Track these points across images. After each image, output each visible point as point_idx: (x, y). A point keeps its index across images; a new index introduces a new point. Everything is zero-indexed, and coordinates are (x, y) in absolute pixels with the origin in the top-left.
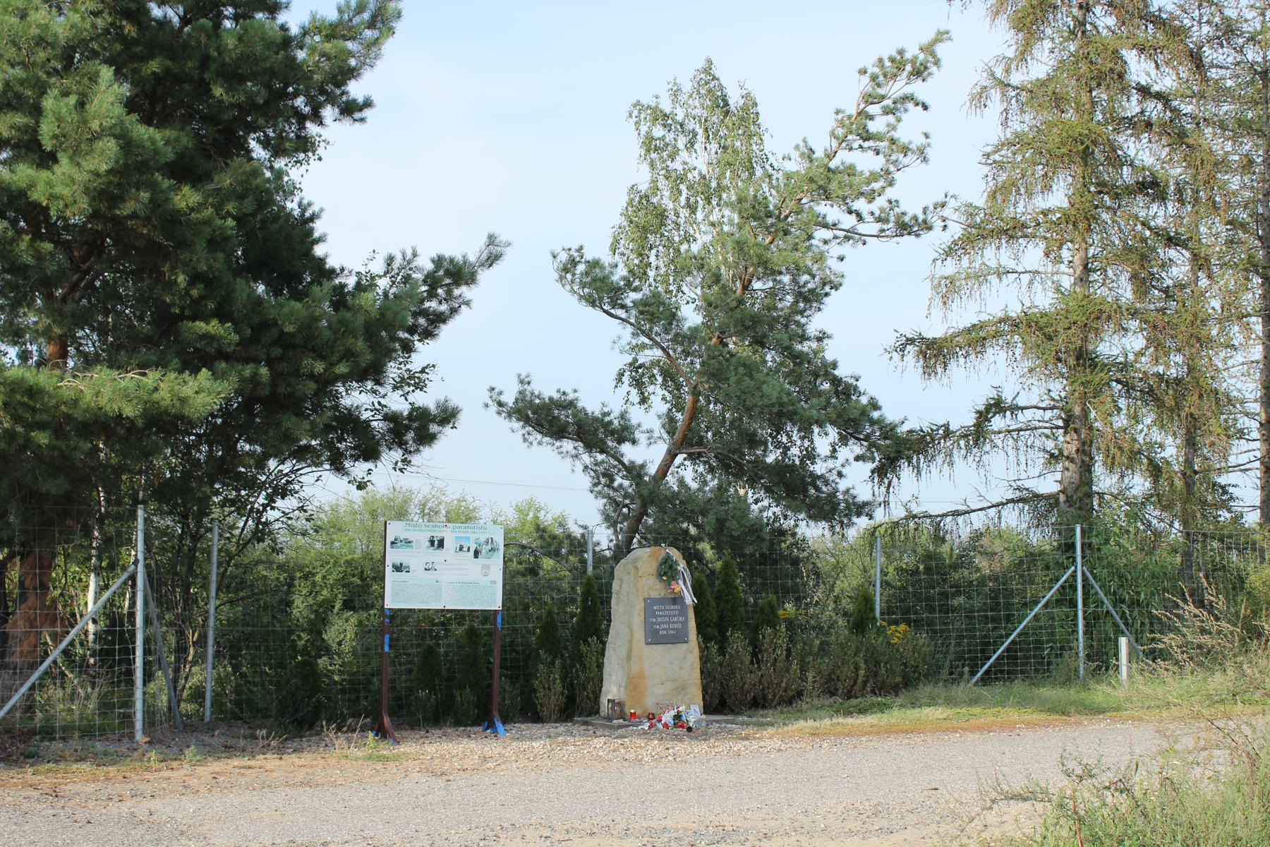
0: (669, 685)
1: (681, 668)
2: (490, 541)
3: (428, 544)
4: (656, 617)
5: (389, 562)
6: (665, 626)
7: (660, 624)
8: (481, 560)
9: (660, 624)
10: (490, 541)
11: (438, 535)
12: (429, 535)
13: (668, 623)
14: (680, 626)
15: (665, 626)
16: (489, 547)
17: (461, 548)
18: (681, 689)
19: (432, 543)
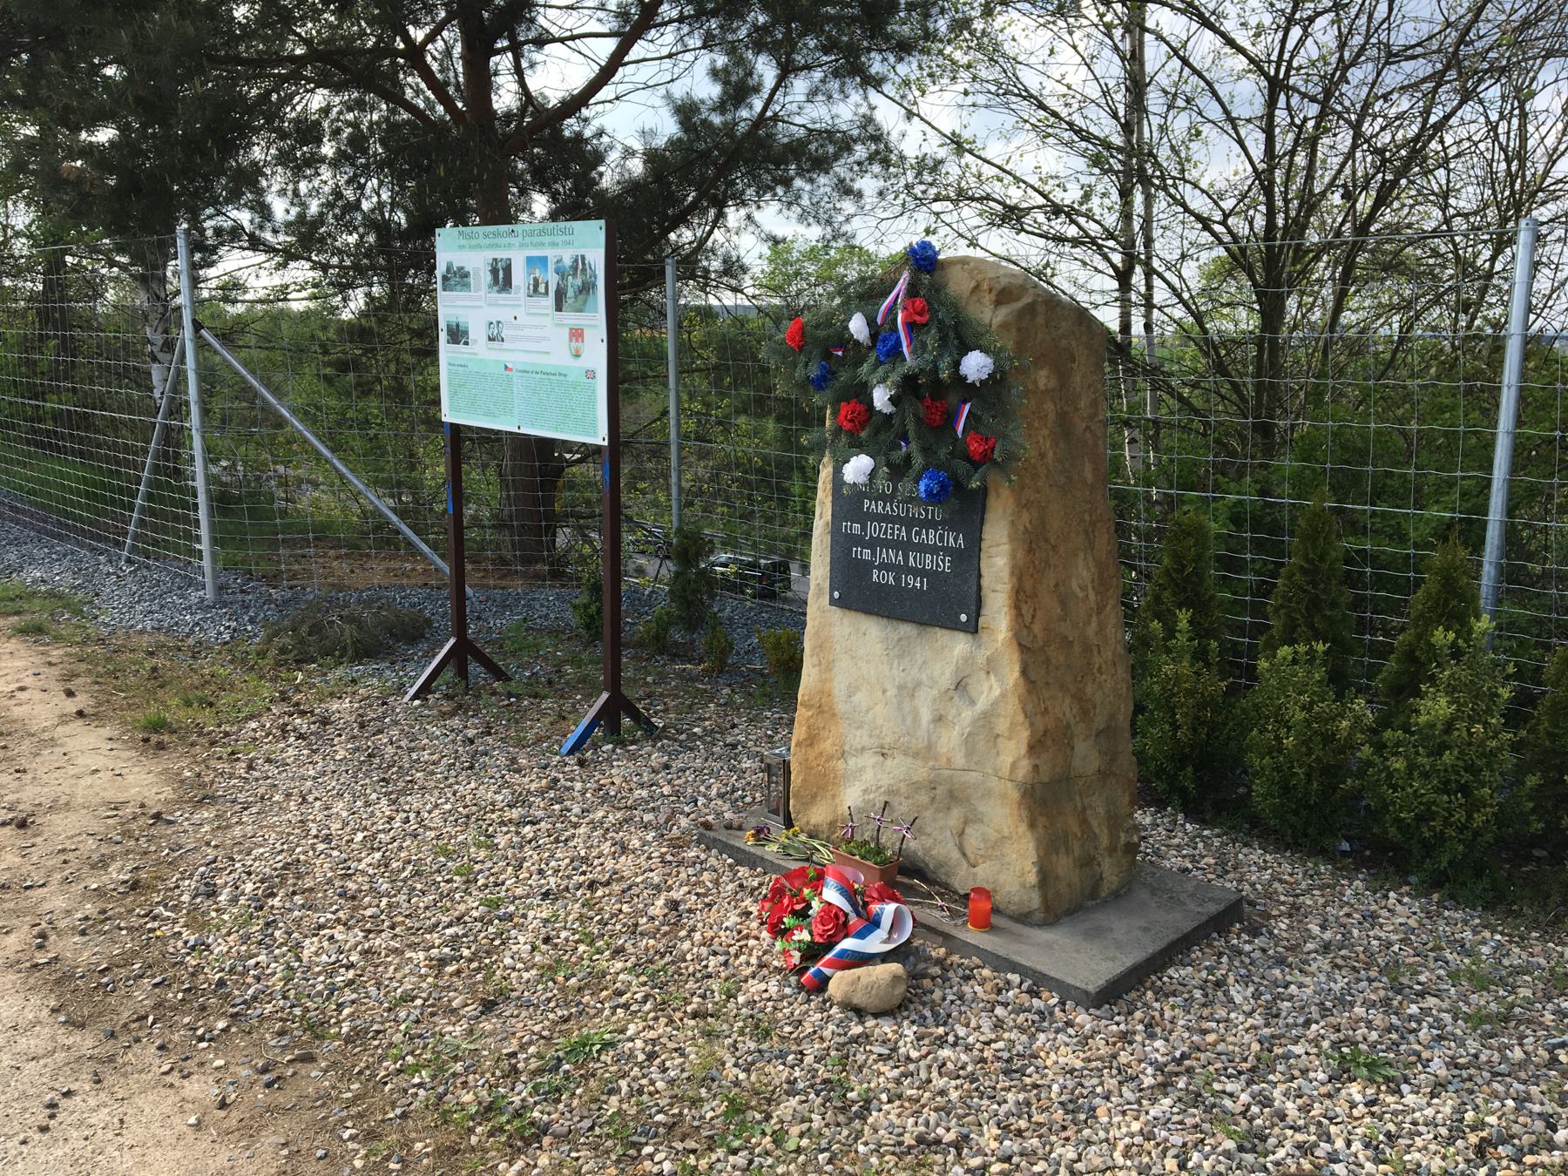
0: (898, 769)
1: (939, 719)
2: (579, 265)
3: (489, 277)
4: (864, 518)
5: (442, 325)
6: (891, 556)
7: (873, 544)
8: (570, 318)
9: (873, 544)
10: (579, 265)
11: (502, 254)
12: (491, 254)
13: (905, 546)
14: (945, 565)
15: (891, 556)
16: (579, 282)
17: (536, 290)
18: (950, 794)
19: (494, 272)
